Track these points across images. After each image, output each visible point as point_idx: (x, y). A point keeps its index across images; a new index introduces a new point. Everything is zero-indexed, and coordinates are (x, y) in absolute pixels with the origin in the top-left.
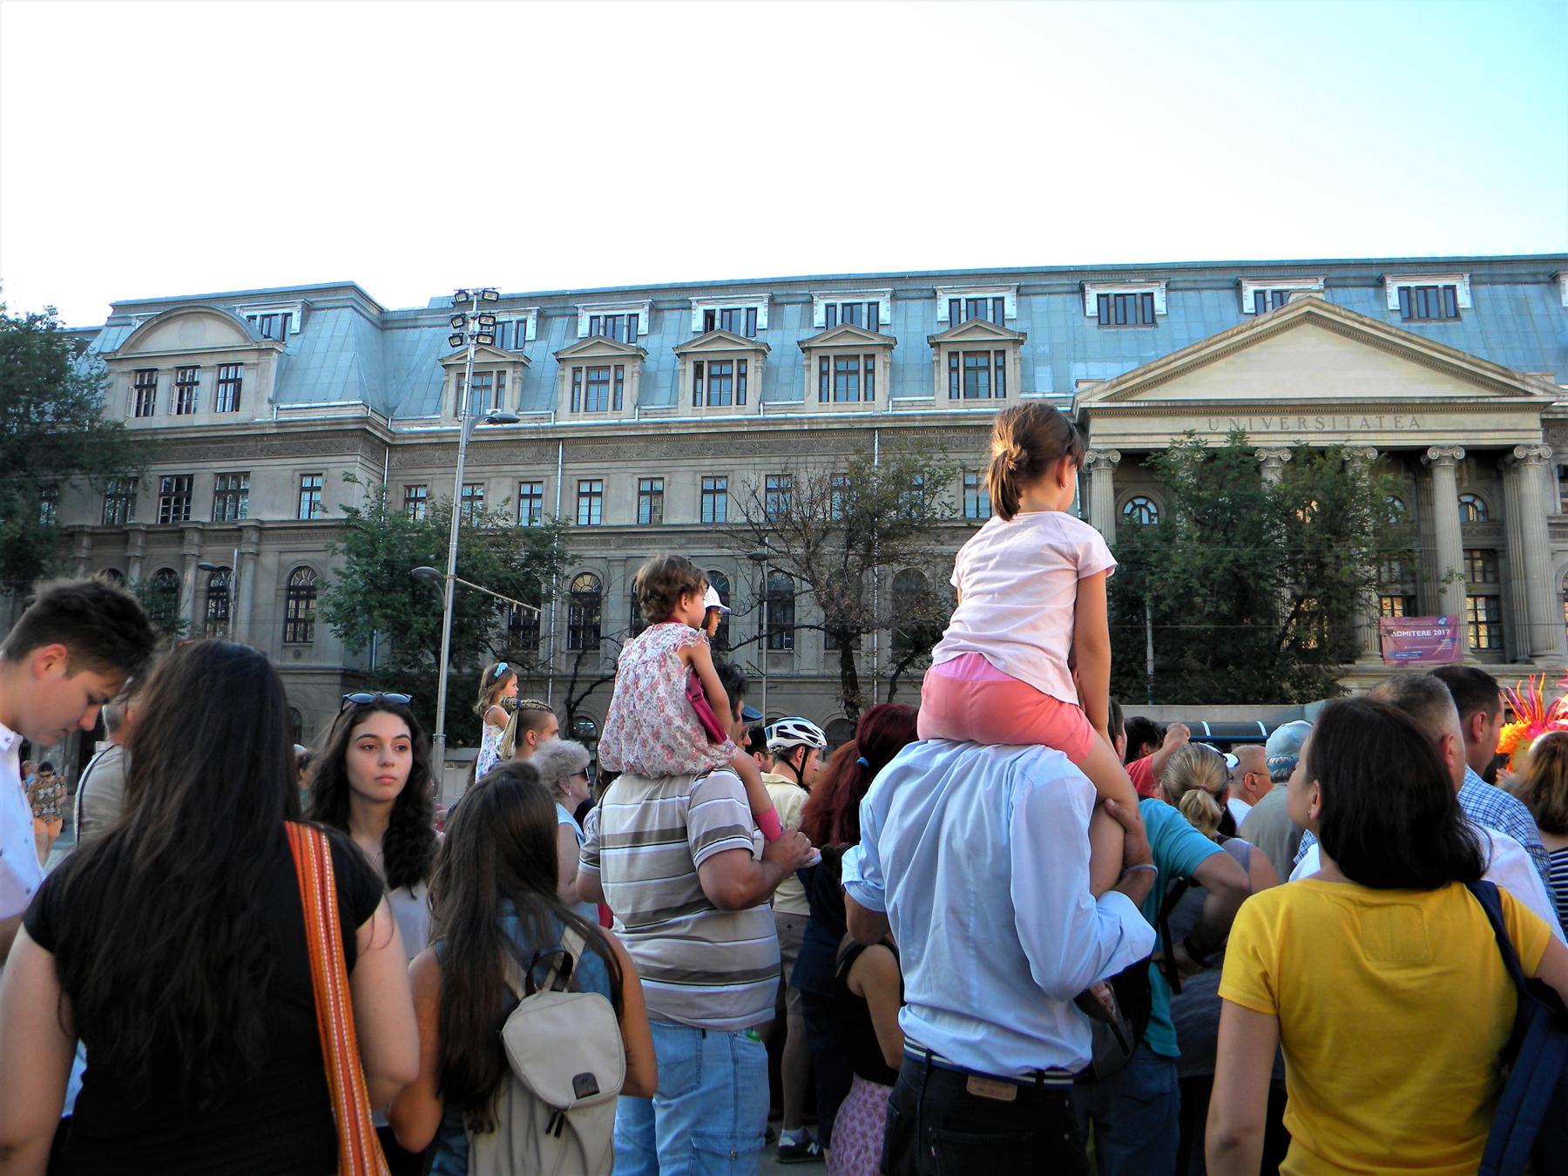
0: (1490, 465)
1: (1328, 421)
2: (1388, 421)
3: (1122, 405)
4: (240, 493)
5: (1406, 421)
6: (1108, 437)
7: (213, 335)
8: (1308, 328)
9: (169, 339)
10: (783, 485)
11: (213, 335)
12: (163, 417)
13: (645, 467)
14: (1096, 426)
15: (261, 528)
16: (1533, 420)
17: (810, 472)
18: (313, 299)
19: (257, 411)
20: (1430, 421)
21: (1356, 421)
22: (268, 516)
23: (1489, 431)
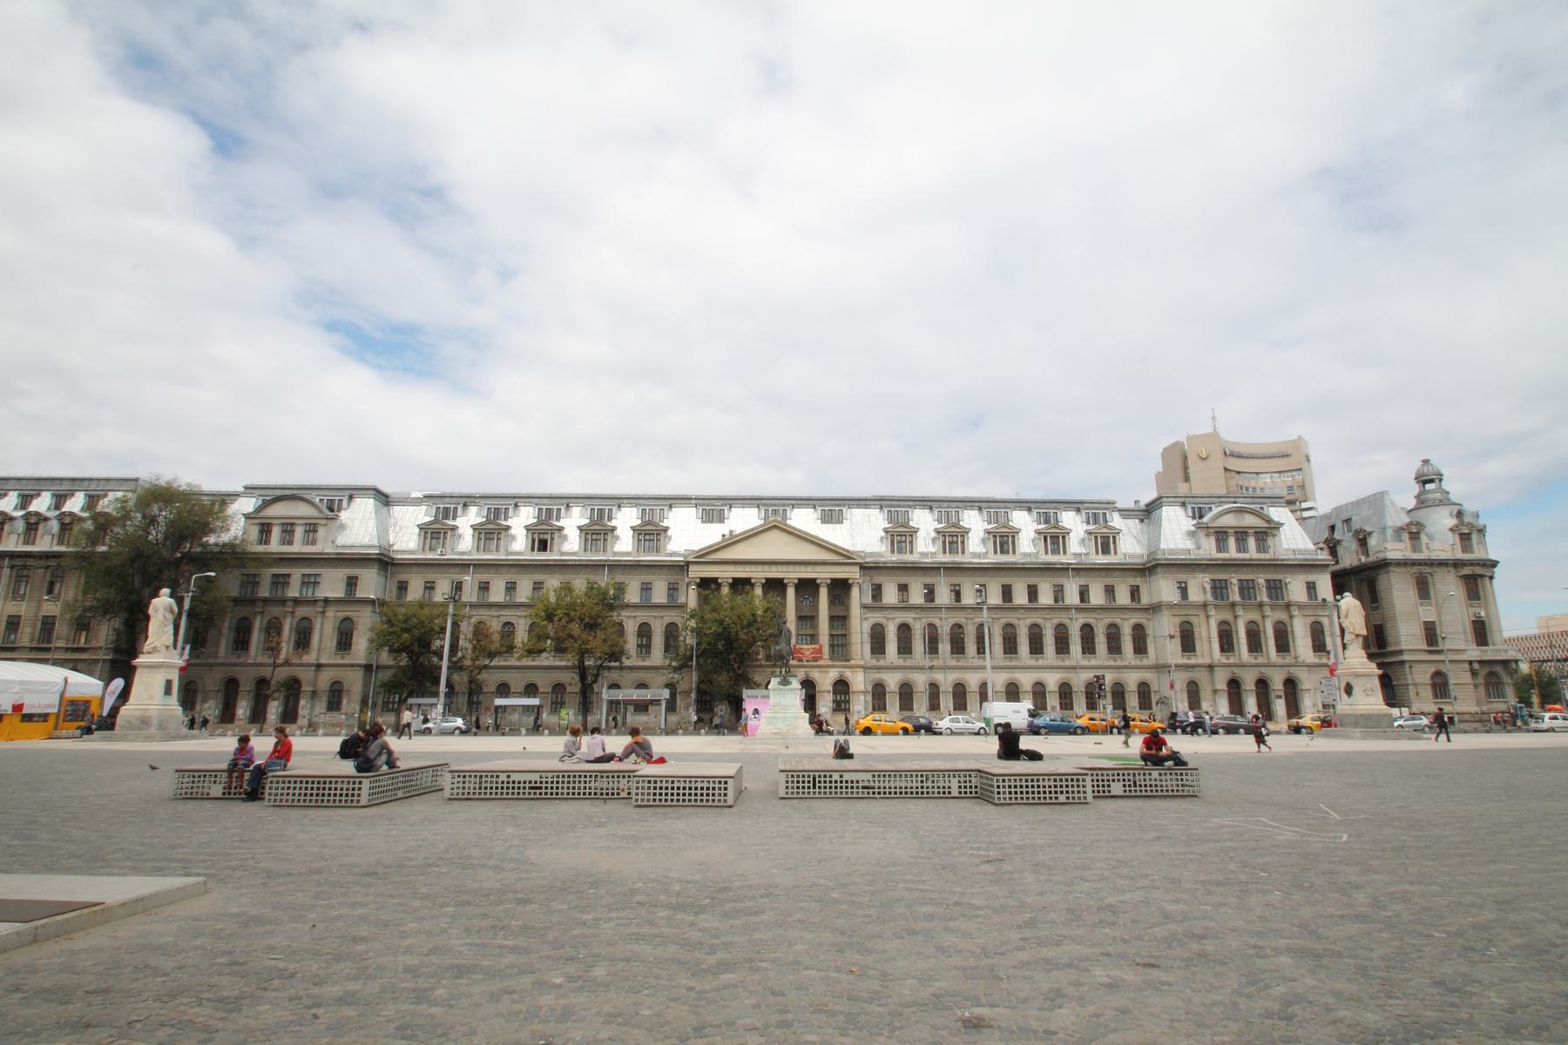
0: (840, 588)
1: (780, 568)
2: (803, 568)
3: (703, 557)
4: (316, 583)
5: (809, 568)
6: (697, 572)
7: (301, 510)
8: (775, 533)
9: (279, 510)
10: (567, 588)
11: (301, 510)
12: (275, 546)
13: (510, 577)
14: (692, 568)
15: (326, 601)
16: (857, 569)
17: (579, 583)
18: (353, 492)
19: (323, 547)
20: (818, 568)
21: (791, 568)
22: (330, 595)
23: (840, 573)
